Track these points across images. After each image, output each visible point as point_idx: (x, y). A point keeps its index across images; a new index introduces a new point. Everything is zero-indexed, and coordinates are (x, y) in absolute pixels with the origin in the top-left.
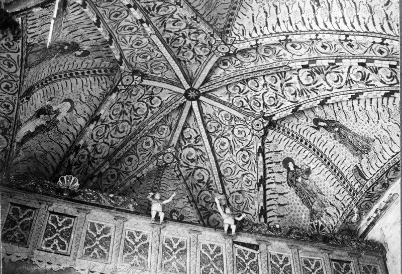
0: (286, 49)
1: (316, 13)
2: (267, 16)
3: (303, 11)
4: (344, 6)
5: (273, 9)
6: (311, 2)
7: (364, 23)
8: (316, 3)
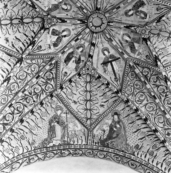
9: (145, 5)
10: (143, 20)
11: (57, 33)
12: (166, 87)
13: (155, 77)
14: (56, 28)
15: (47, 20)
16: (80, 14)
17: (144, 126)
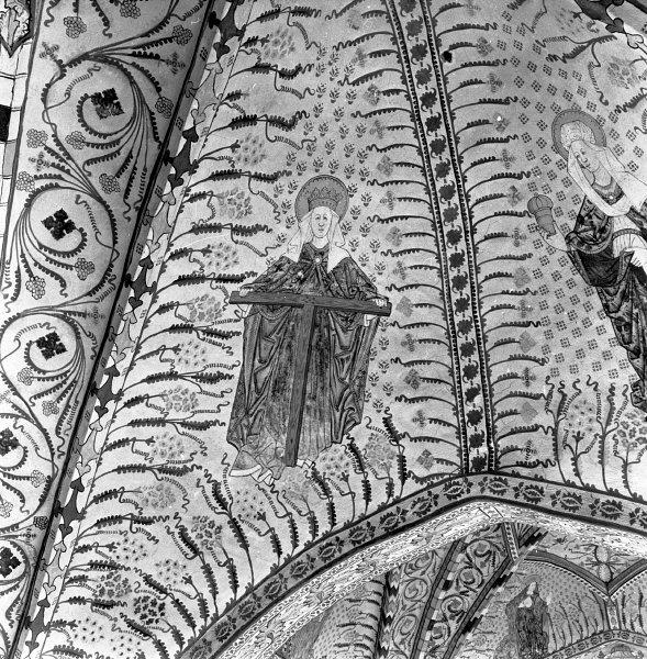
0: (102, 57)
1: (214, 284)
2: (283, 74)
3: (239, 238)
4: (207, 387)
5: (286, 107)
6: (254, 274)
7: (134, 440)
8: (244, 292)
12: (483, 581)
13: (487, 549)
17: (371, 622)
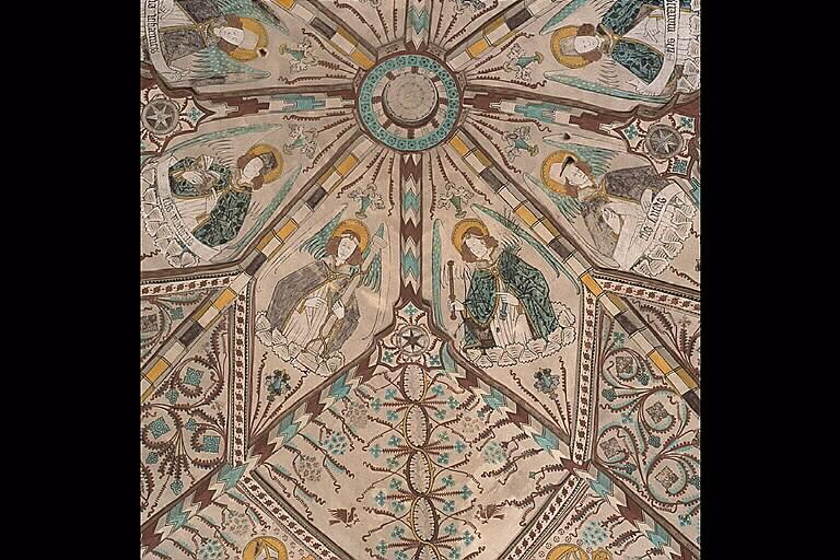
9: (194, 233)
10: (181, 155)
11: (631, 52)
14: (632, 82)
15: (676, 147)
16: (502, 133)
